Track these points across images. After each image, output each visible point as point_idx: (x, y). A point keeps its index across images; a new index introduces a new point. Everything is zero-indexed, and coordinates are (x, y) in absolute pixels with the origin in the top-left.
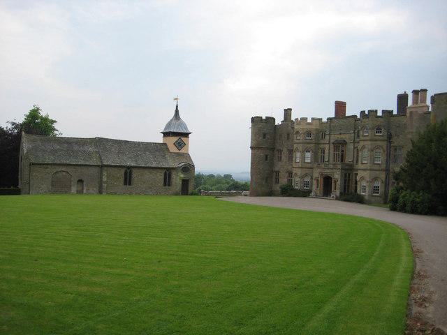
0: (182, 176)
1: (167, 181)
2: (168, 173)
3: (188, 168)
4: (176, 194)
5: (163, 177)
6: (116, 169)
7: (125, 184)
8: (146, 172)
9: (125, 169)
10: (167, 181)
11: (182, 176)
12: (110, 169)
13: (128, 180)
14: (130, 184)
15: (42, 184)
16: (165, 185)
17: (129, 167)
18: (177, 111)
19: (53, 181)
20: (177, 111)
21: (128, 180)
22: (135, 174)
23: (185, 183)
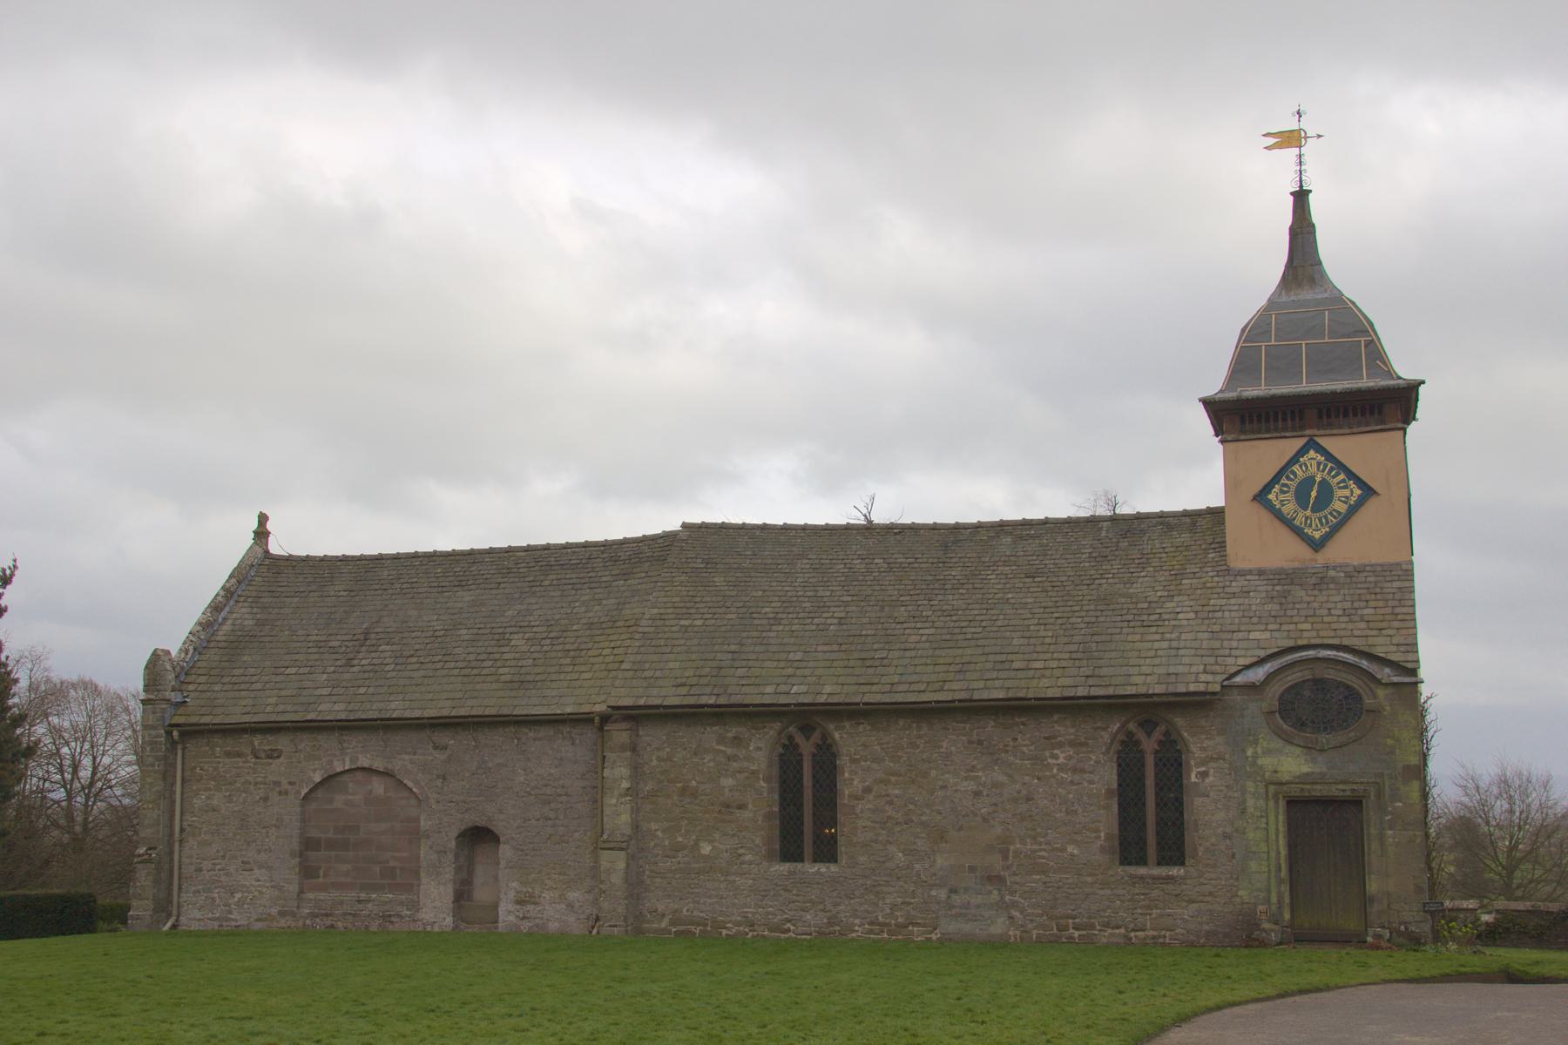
0: (1292, 764)
1: (1151, 823)
2: (1149, 748)
3: (1355, 691)
4: (1245, 935)
5: (1108, 776)
6: (709, 735)
7: (790, 850)
8: (953, 739)
9: (772, 730)
10: (1151, 823)
11: (1292, 764)
12: (652, 736)
13: (806, 820)
14: (827, 851)
15: (246, 866)
16: (1130, 849)
17: (807, 718)
18: (1302, 231)
19: (309, 844)
20: (1302, 231)
21: (806, 820)
22: (862, 765)
23: (1325, 826)
